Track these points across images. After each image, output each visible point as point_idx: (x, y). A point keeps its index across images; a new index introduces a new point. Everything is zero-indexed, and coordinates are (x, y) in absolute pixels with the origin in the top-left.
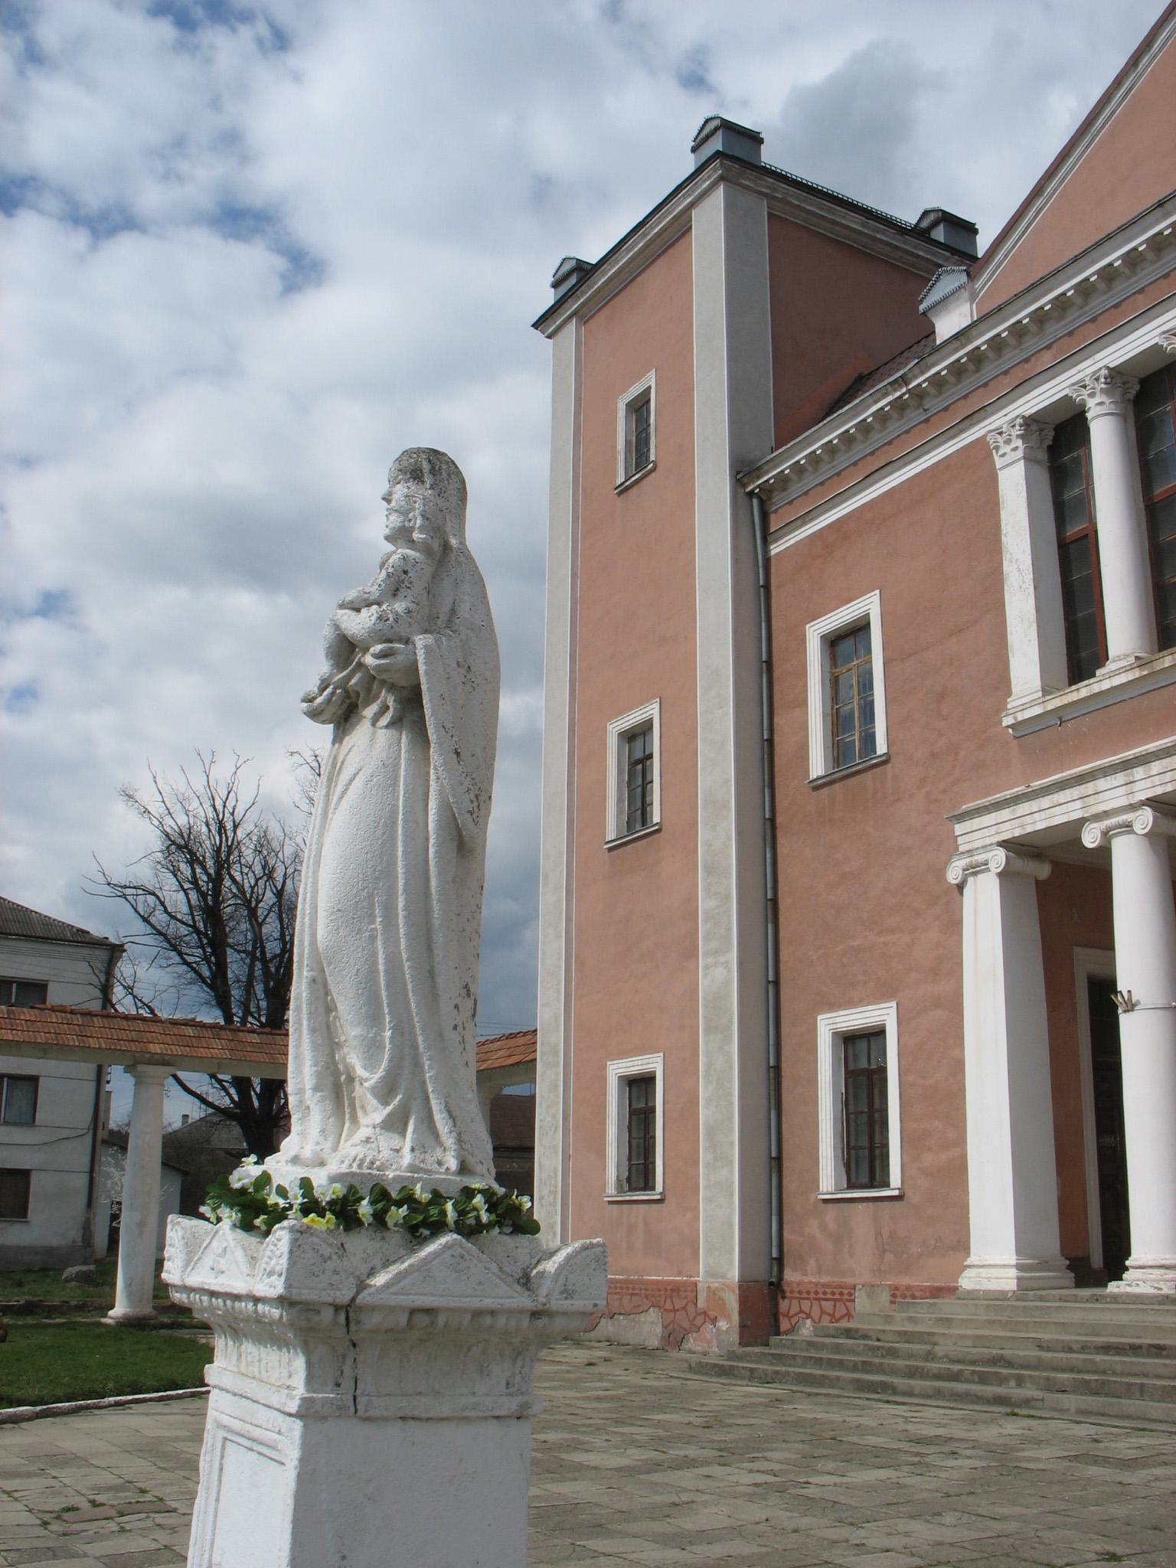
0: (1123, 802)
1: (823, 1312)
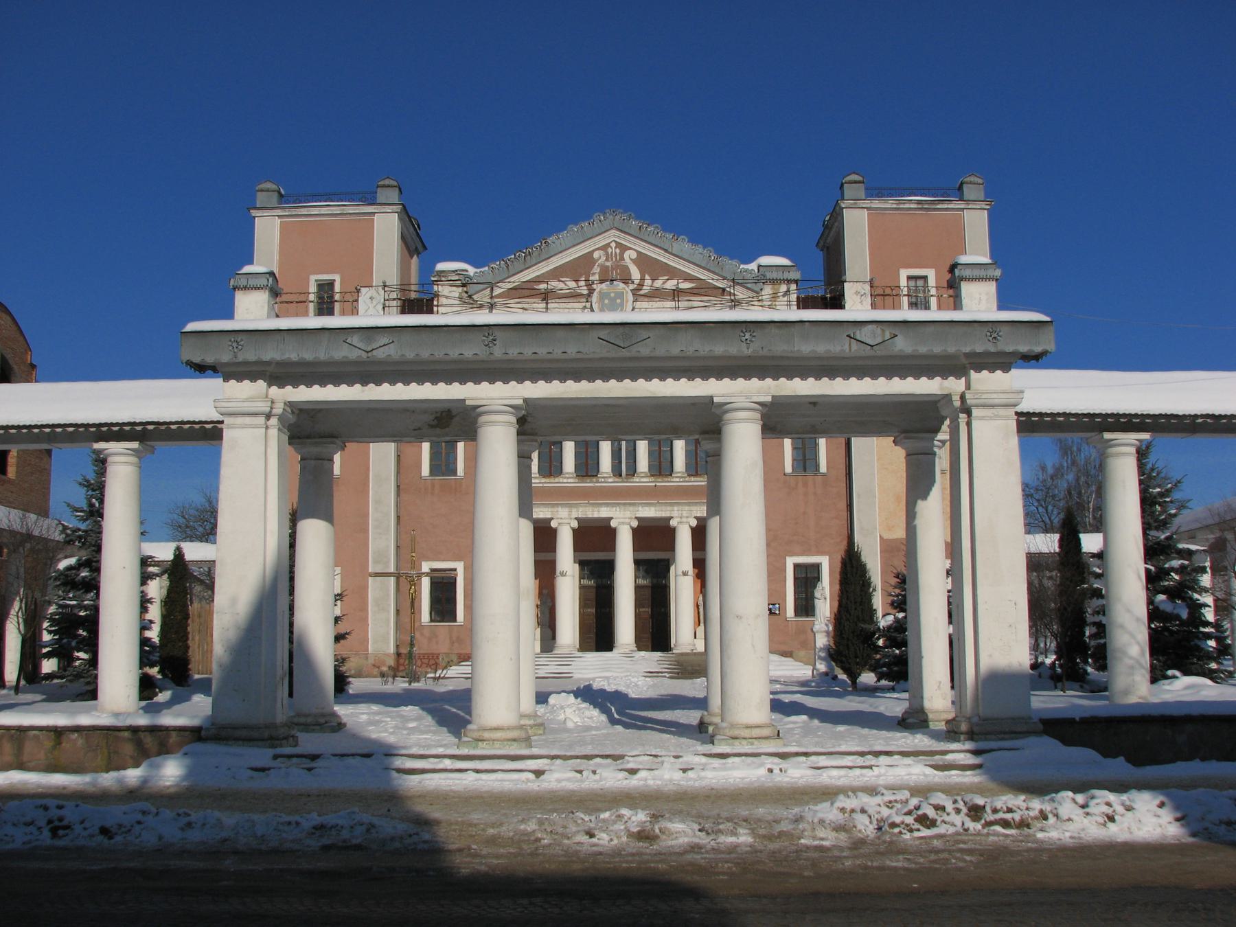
0: (567, 516)
1: (422, 663)
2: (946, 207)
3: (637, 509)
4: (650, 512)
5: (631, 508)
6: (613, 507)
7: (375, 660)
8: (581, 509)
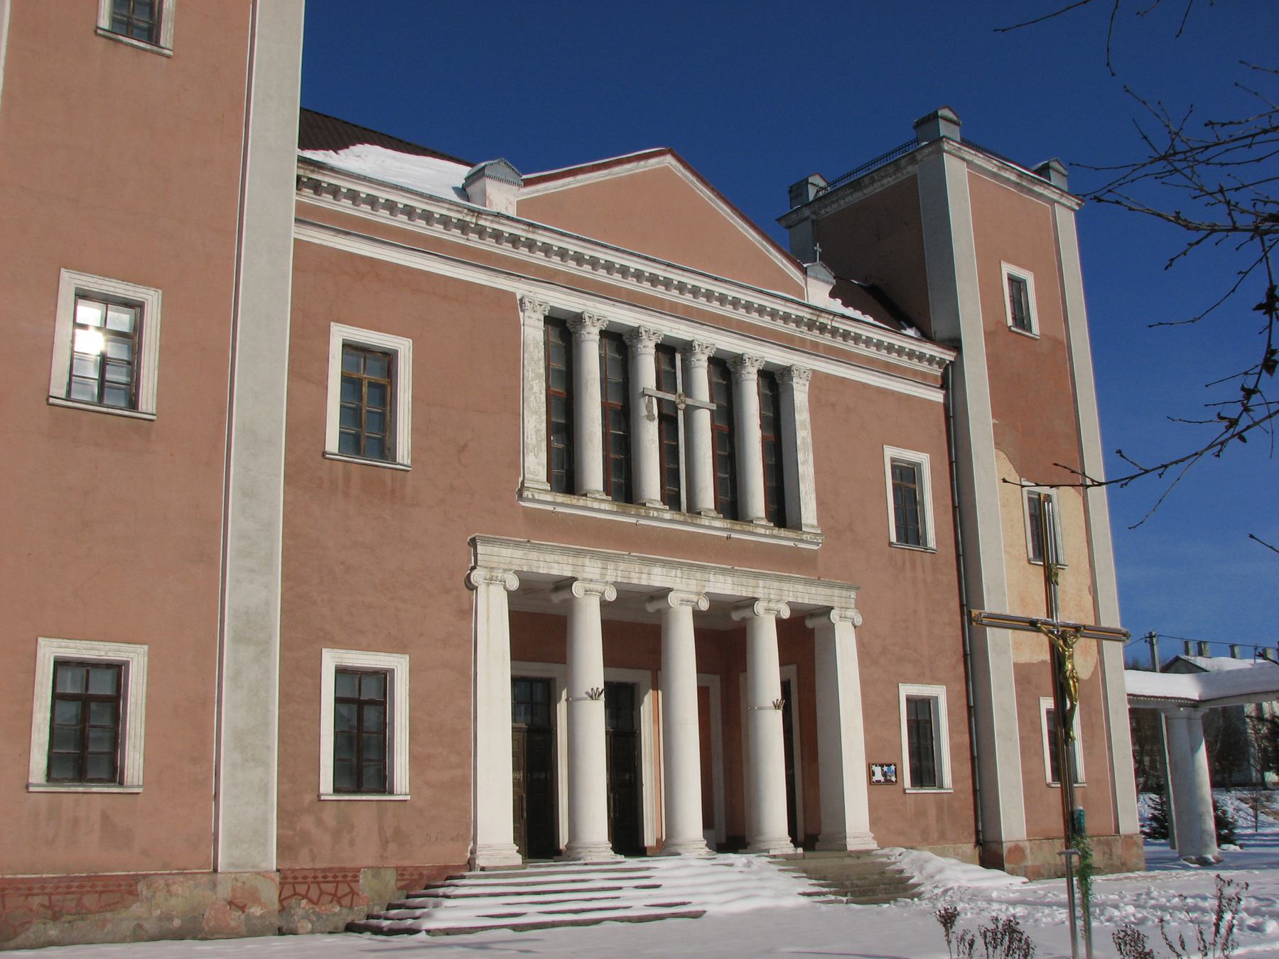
0: (598, 577)
1: (322, 893)
2: (1041, 192)
3: (707, 575)
4: (726, 586)
5: (699, 575)
6: (673, 568)
7: (234, 889)
8: (622, 566)
